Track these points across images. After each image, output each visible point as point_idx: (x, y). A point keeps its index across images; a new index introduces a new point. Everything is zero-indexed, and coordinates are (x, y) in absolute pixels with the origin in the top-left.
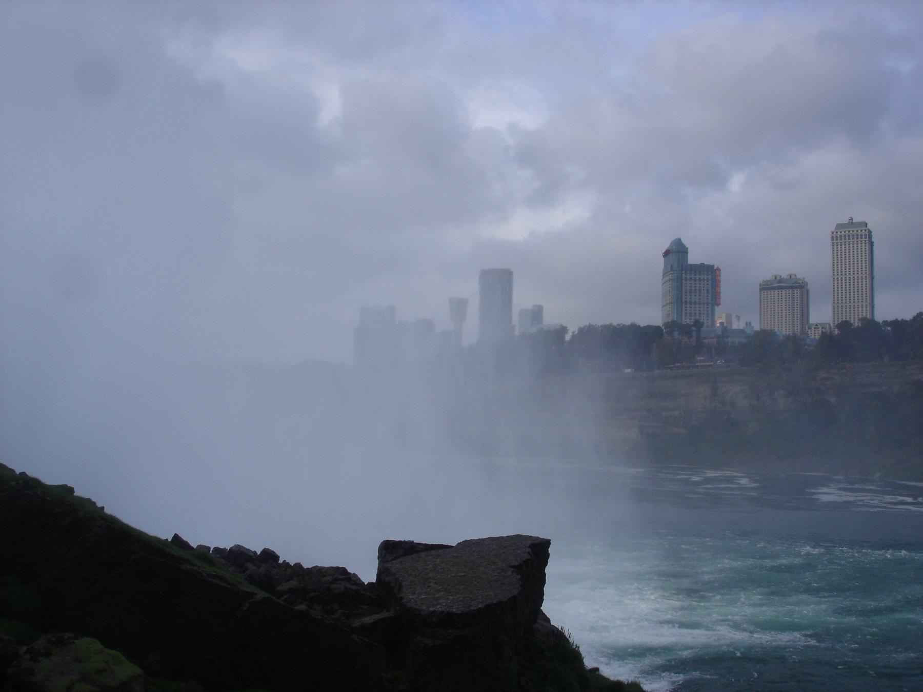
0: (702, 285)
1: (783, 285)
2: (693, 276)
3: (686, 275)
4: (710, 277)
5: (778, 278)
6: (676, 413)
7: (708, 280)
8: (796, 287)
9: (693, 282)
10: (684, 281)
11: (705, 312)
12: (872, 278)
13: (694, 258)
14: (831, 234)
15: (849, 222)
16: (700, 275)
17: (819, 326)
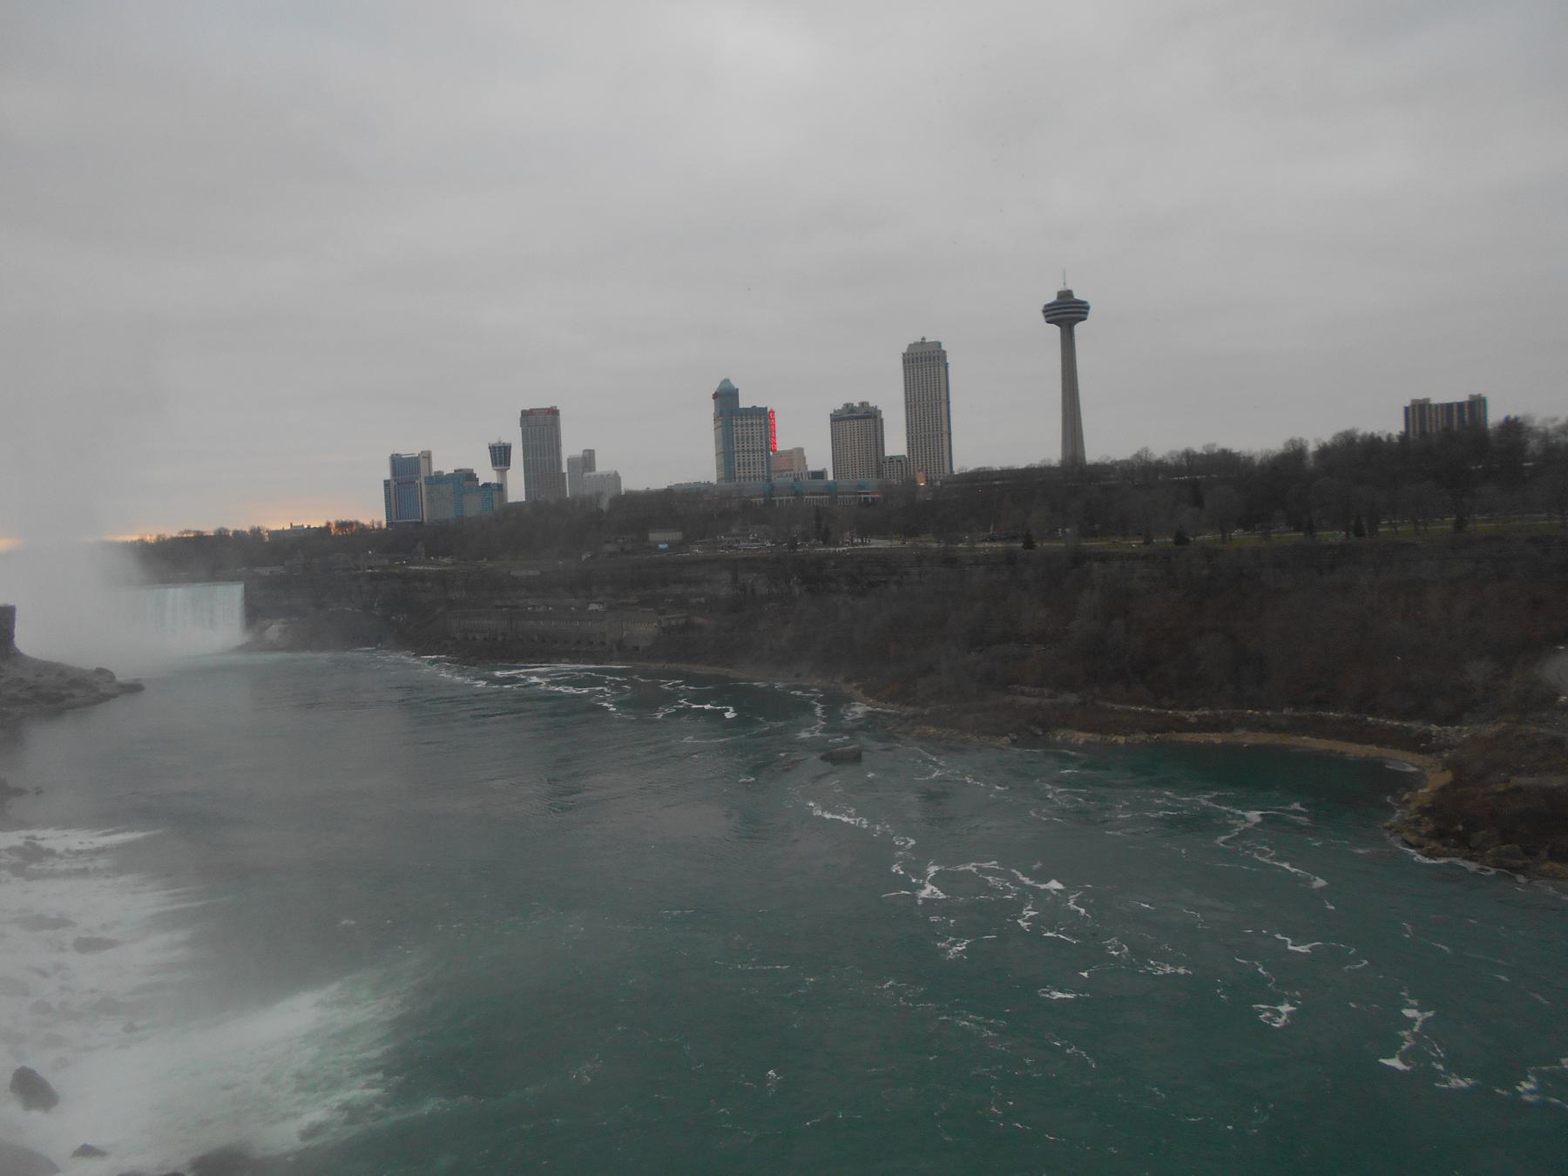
0: (755, 431)
1: (855, 415)
2: (744, 422)
3: (736, 420)
4: (762, 421)
5: (850, 407)
6: (702, 600)
7: (761, 425)
8: (869, 417)
9: (745, 428)
10: (735, 429)
11: (760, 460)
12: (948, 403)
13: (744, 403)
14: (902, 356)
15: (921, 343)
16: (752, 418)
17: (895, 460)
